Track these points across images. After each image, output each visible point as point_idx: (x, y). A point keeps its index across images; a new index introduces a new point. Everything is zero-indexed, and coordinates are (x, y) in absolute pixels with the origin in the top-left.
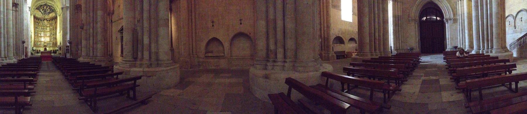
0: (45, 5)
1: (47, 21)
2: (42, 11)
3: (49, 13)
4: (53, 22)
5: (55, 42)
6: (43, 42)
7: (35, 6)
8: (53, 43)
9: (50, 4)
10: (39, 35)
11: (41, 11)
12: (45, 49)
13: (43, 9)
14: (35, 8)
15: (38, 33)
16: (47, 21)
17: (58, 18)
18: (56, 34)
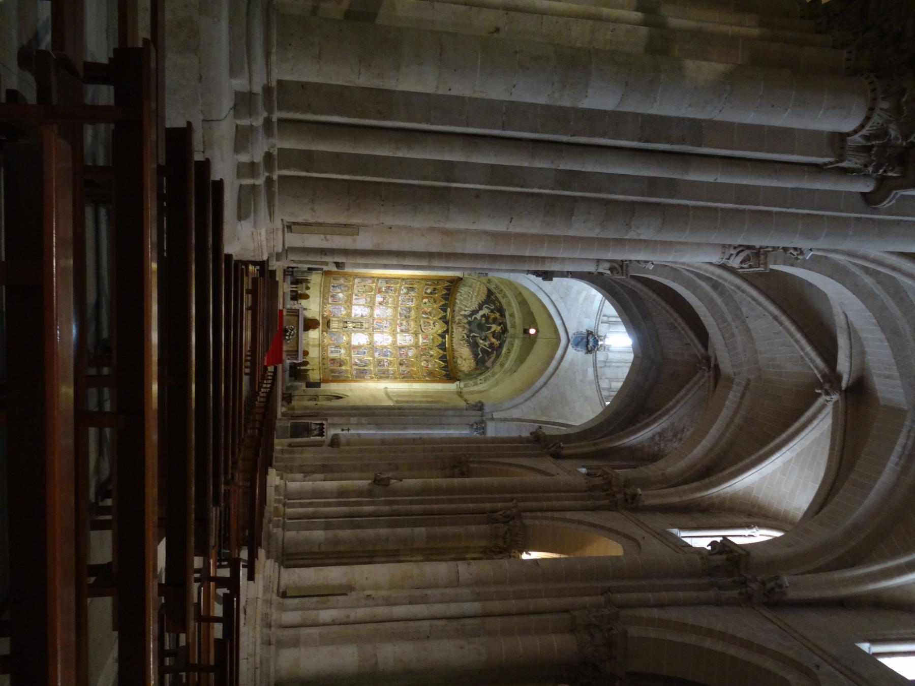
0: (505, 326)
1: (439, 335)
3: (474, 346)
4: (435, 364)
5: (346, 371)
6: (349, 315)
8: (341, 363)
9: (509, 351)
10: (379, 299)
11: (480, 307)
12: (311, 324)
13: (491, 321)
14: (492, 287)
15: (386, 292)
16: (442, 336)
17: (452, 387)
18: (381, 378)
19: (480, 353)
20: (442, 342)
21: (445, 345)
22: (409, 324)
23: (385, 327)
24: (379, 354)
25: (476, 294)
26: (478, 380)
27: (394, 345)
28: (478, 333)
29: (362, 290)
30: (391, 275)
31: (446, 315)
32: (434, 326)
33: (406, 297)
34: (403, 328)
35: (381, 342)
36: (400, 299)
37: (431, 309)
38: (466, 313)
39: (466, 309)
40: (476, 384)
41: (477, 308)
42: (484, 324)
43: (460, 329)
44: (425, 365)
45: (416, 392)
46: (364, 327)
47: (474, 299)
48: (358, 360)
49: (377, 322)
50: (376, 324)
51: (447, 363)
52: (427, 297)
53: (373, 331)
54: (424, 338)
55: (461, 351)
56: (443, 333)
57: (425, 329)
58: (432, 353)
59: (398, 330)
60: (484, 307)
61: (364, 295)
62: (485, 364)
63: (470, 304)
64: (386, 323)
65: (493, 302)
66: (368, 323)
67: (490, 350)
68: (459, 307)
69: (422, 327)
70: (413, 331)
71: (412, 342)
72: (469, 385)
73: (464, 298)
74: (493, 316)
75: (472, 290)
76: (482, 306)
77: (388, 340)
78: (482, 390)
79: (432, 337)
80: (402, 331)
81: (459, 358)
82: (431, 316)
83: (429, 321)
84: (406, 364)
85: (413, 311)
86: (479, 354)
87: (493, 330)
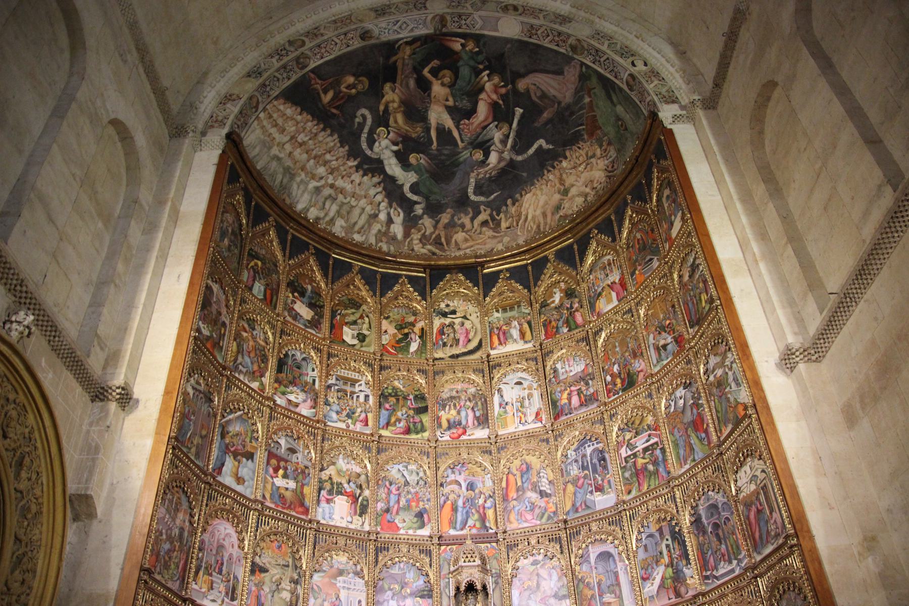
2: (393, 168)
7: (265, 49)
13: (416, 131)
15: (301, 474)
19: (531, 151)
20: (508, 279)
21: (527, 265)
22: (452, 398)
23: (471, 487)
24: (599, 489)
25: (321, 170)
26: (633, 70)
27: (547, 441)
28: (468, 174)
29: (286, 585)
30: (167, 392)
31: (407, 276)
32: (454, 312)
33: (332, 398)
34: (467, 417)
35: (542, 494)
36: (343, 426)
37: (385, 324)
38: (399, 219)
39: (382, 216)
40: (655, 74)
41: (376, 180)
42: (431, 157)
43: (460, 236)
44: (614, 294)
45: (763, 235)
46: (477, 577)
47: (340, 183)
48: (644, 579)
49: (452, 524)
50: (462, 529)
51: (589, 232)
52: (332, 327)
53: (494, 538)
54: (504, 337)
55: (534, 217)
56: (476, 284)
57: (469, 341)
58: (557, 298)
59: (481, 434)
60: (368, 152)
61: (317, 577)
62: (568, 107)
63: (363, 202)
64: (455, 487)
65: (347, 104)
66: (456, 561)
67: (519, 111)
68: (379, 240)
69: (456, 351)
70: (478, 379)
71: (520, 374)
72: (664, 91)
73: (338, 212)
74: (400, 118)
75: (303, 175)
76: (366, 160)
77: (529, 467)
78: (668, 50)
79: (496, 315)
80: (483, 420)
81: (561, 213)
82: (413, 324)
83: (435, 331)
84: (625, 365)
85: (396, 383)
86: (541, 146)
87: (449, 123)
